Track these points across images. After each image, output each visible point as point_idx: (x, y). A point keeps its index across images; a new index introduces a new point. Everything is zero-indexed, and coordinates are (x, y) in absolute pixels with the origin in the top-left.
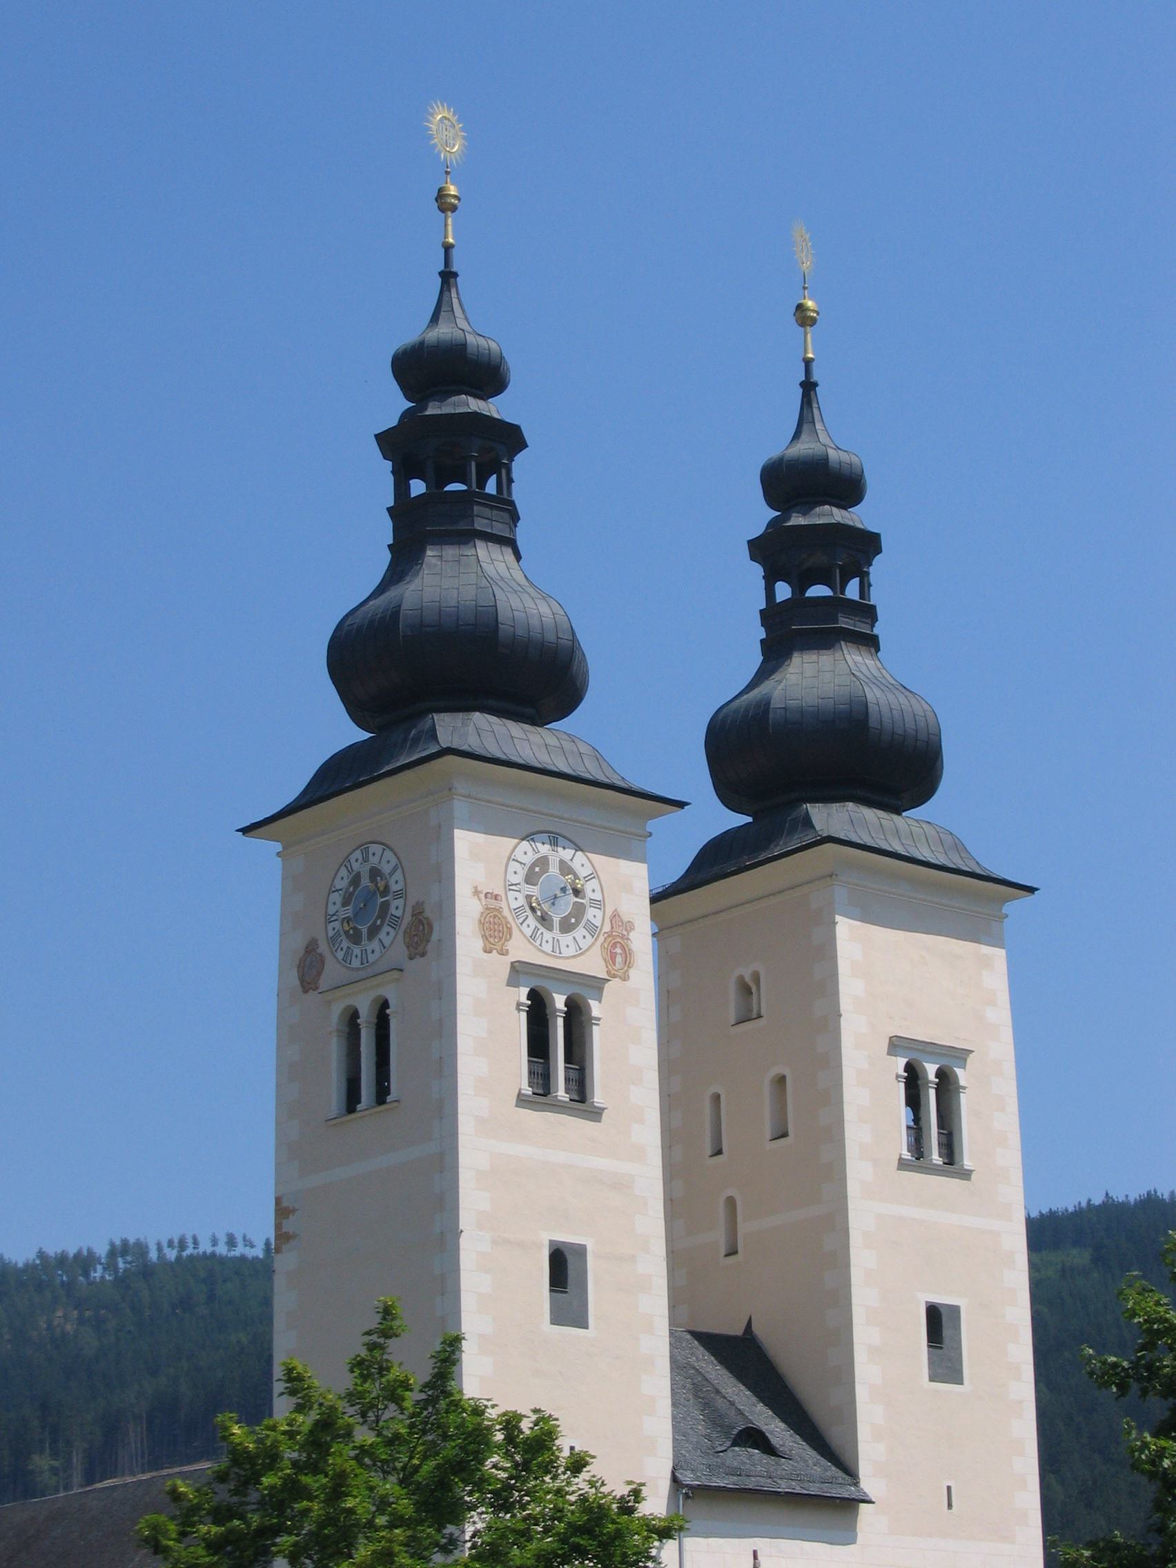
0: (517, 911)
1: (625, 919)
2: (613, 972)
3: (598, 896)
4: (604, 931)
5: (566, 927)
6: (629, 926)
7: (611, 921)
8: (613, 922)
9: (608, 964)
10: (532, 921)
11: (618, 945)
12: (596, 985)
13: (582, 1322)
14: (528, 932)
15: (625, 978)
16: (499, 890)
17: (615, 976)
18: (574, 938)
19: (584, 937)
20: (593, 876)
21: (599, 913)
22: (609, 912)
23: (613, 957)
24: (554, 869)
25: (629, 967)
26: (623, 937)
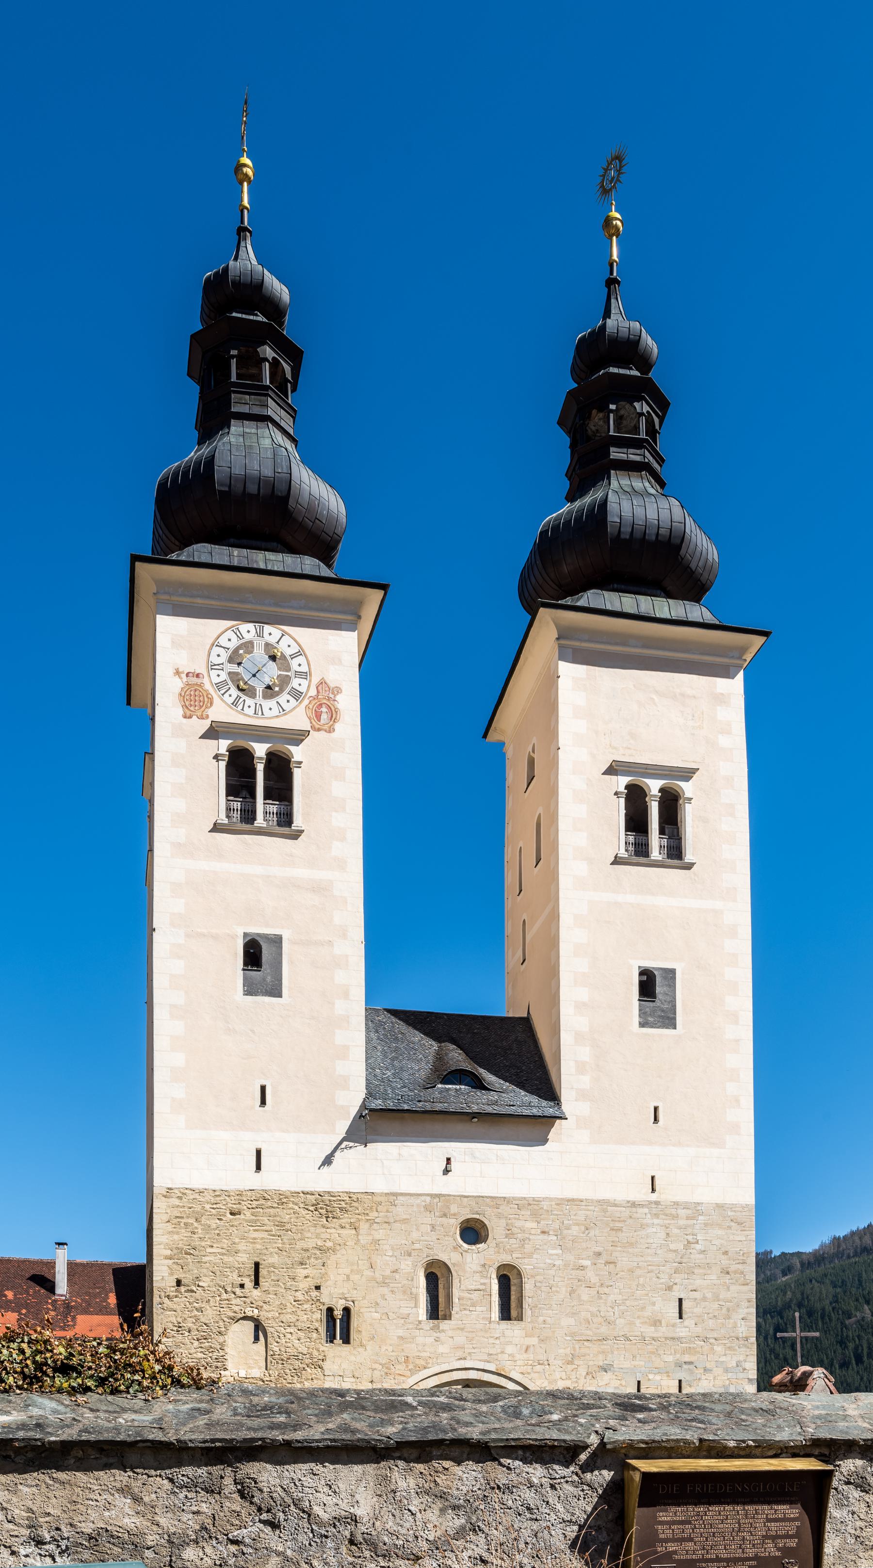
1: (332, 685)
2: (317, 726)
3: (304, 668)
4: (309, 694)
6: (338, 690)
7: (317, 688)
8: (320, 688)
9: (312, 721)
11: (324, 706)
12: (298, 737)
13: (275, 991)
15: (331, 730)
17: (319, 730)
18: (277, 702)
19: (288, 701)
20: (300, 653)
21: (305, 683)
22: (315, 680)
23: (318, 716)
24: (259, 654)
25: (334, 721)
26: (329, 699)
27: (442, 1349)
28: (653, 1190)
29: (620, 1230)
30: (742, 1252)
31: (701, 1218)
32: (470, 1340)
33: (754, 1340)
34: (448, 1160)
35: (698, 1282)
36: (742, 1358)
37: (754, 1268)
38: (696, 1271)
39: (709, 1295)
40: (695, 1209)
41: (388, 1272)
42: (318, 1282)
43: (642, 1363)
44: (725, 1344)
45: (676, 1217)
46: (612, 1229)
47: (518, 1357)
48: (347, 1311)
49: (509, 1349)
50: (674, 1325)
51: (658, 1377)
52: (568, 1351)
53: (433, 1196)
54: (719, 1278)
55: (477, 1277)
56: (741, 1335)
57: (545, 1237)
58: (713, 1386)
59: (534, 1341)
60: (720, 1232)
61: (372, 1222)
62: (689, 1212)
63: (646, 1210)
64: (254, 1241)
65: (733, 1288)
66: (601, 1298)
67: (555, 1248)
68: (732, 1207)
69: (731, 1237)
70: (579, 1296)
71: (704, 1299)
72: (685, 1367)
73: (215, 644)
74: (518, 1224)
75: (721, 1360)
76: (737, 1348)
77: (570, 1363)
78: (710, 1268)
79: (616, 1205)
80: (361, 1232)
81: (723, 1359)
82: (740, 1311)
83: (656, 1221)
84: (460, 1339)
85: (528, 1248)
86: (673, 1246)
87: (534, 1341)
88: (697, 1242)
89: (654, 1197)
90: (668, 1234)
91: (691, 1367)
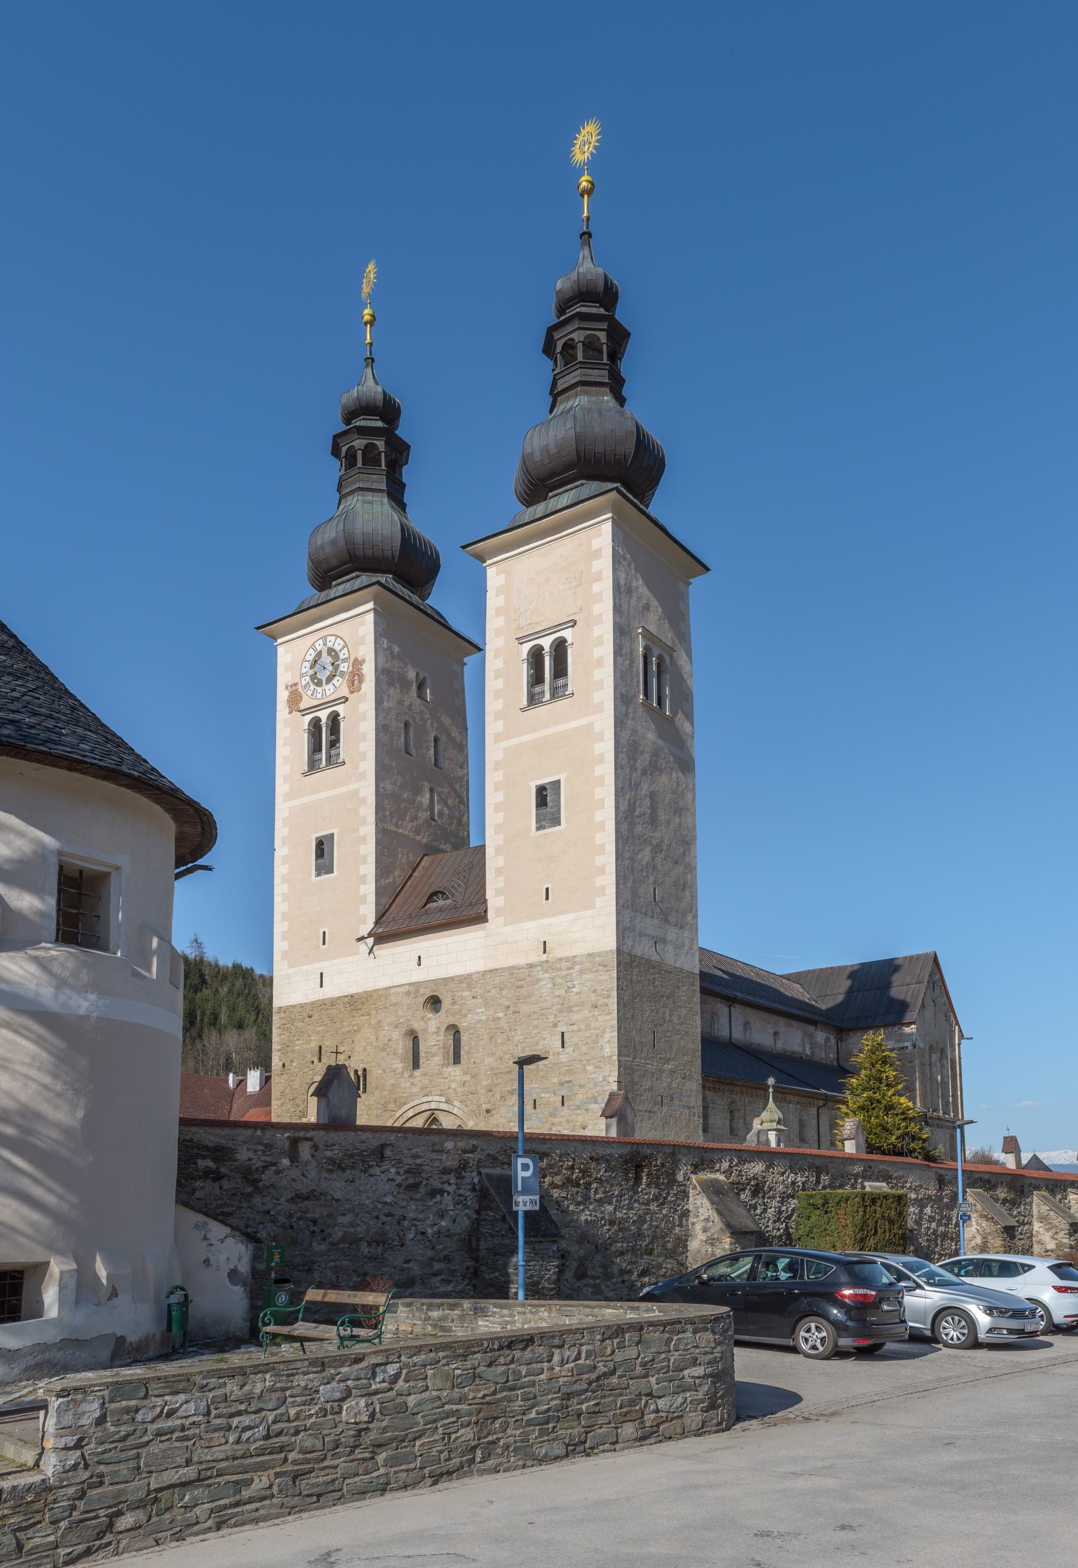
0: (305, 686)
1: (360, 659)
5: (329, 680)
6: (364, 661)
10: (312, 687)
14: (309, 693)
15: (359, 690)
16: (297, 680)
17: (353, 692)
20: (344, 647)
21: (346, 664)
22: (352, 660)
23: (353, 685)
27: (415, 1090)
28: (545, 952)
29: (522, 986)
32: (431, 1081)
33: (615, 1058)
34: (419, 957)
35: (575, 1017)
36: (607, 1074)
37: (615, 1000)
38: (574, 1009)
39: (583, 1027)
40: (572, 961)
41: (386, 1042)
42: (350, 1054)
43: (537, 1086)
44: (594, 1064)
45: (560, 969)
46: (517, 987)
47: (458, 1090)
48: (365, 1070)
49: (453, 1085)
50: (558, 1053)
51: (547, 1095)
52: (489, 1082)
53: (410, 984)
54: (590, 1011)
55: (434, 1036)
56: (606, 1055)
57: (475, 1000)
59: (468, 1077)
60: (591, 976)
61: (377, 1009)
62: (569, 963)
63: (540, 968)
64: (318, 1033)
65: (599, 1018)
66: (509, 1040)
67: (480, 1008)
68: (599, 954)
69: (599, 978)
70: (496, 1040)
71: (579, 1030)
72: (566, 1085)
73: (304, 660)
74: (458, 994)
77: (490, 1090)
78: (583, 1005)
79: (519, 969)
80: (372, 1016)
81: (594, 1076)
82: (606, 1035)
83: (546, 975)
84: (426, 1081)
85: (464, 1012)
86: (557, 993)
87: (468, 1077)
89: (544, 957)
90: (554, 984)
91: (570, 1084)
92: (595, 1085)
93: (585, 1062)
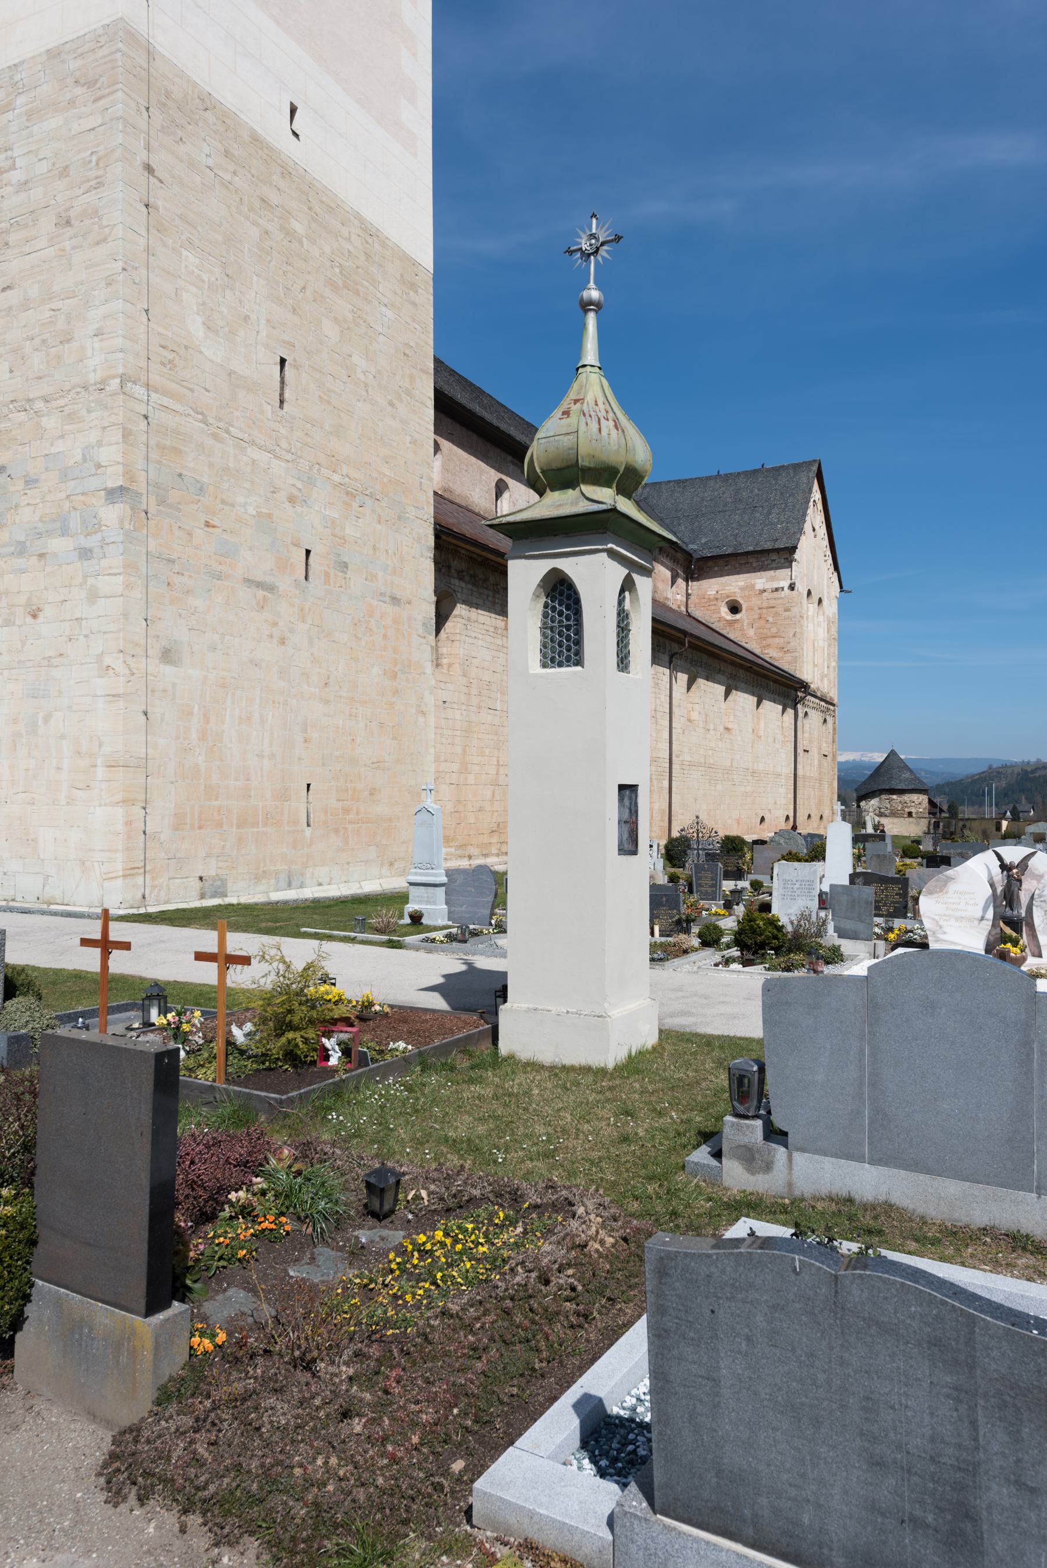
30: (94, 158)
31: (21, 100)
38: (12, 238)
58: (41, 520)
71: (26, 305)
75: (54, 450)
76: (84, 412)
81: (59, 447)
88: (13, 167)
92: (65, 475)
93: (39, 405)
